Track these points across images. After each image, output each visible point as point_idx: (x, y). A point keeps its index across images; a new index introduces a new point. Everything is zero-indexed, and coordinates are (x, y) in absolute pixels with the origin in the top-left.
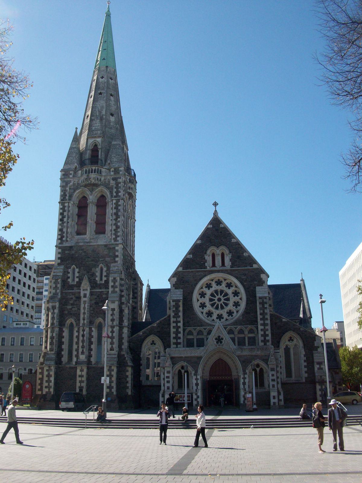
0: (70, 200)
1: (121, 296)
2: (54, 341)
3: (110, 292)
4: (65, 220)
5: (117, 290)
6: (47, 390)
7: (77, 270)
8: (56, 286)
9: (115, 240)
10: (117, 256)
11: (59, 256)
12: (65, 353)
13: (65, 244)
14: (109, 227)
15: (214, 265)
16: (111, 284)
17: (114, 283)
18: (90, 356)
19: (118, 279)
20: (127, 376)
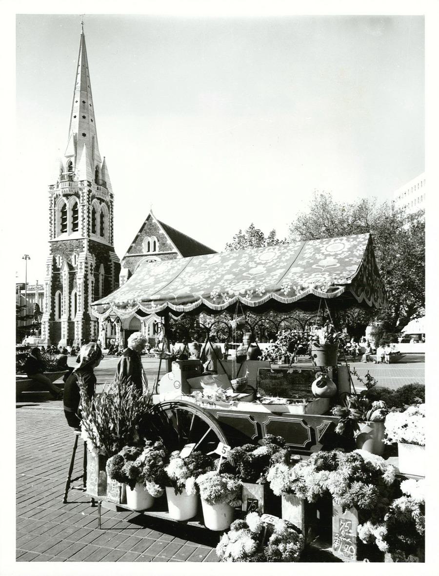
0: (55, 207)
1: (86, 276)
2: (48, 305)
3: (78, 273)
4: (53, 222)
5: (83, 271)
6: (44, 336)
7: (61, 258)
8: (48, 270)
9: (82, 235)
10: (84, 247)
11: (50, 248)
12: (57, 313)
13: (54, 240)
14: (80, 226)
15: (149, 251)
16: (79, 267)
17: (81, 266)
18: (70, 315)
19: (83, 264)
20: (91, 327)
